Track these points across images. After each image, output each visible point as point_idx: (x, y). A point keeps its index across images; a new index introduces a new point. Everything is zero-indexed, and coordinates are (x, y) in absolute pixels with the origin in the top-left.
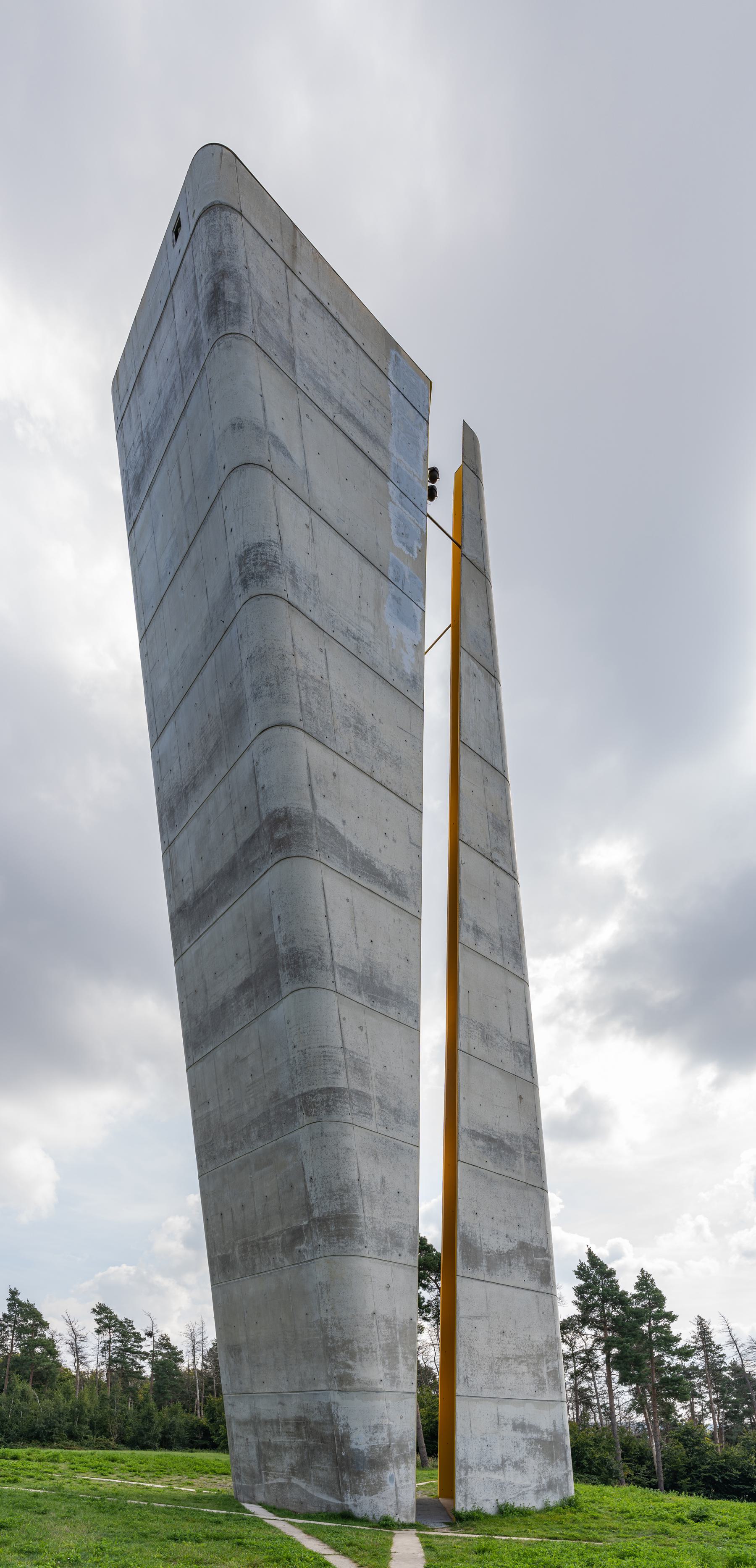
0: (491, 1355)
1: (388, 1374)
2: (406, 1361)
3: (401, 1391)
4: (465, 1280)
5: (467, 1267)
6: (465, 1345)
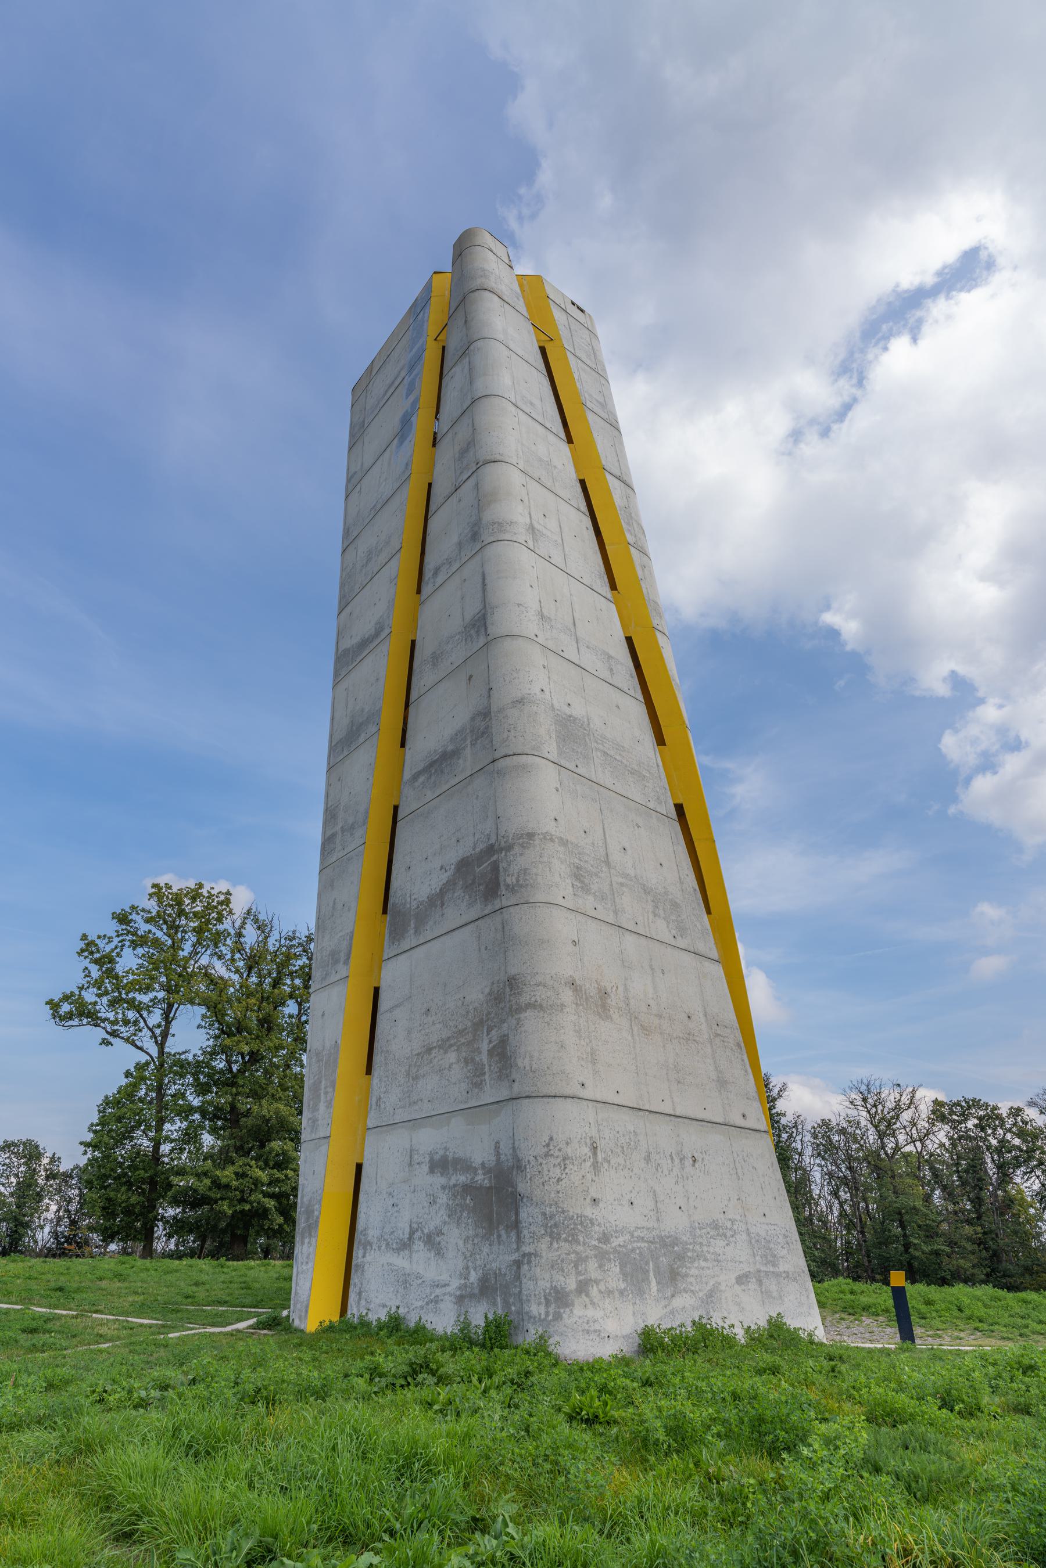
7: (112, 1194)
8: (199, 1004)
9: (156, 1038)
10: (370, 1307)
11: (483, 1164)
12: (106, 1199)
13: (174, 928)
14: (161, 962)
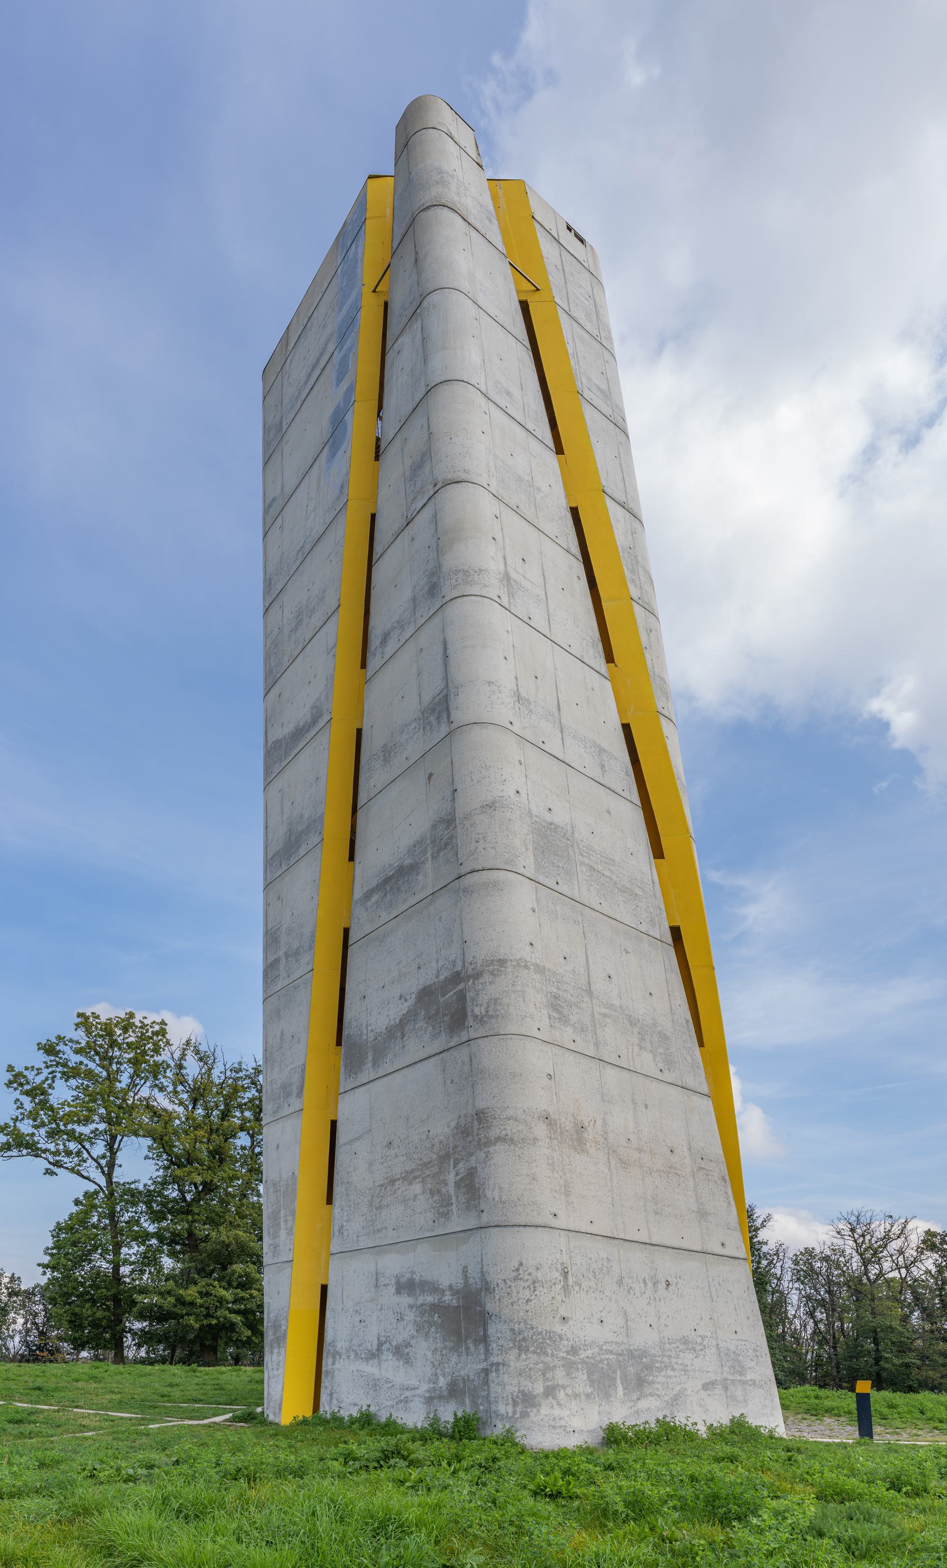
7: (77, 1310)
8: (144, 1136)
9: (102, 1168)
10: (342, 1406)
11: (451, 1287)
12: (72, 1314)
13: (107, 1060)
14: (98, 1094)
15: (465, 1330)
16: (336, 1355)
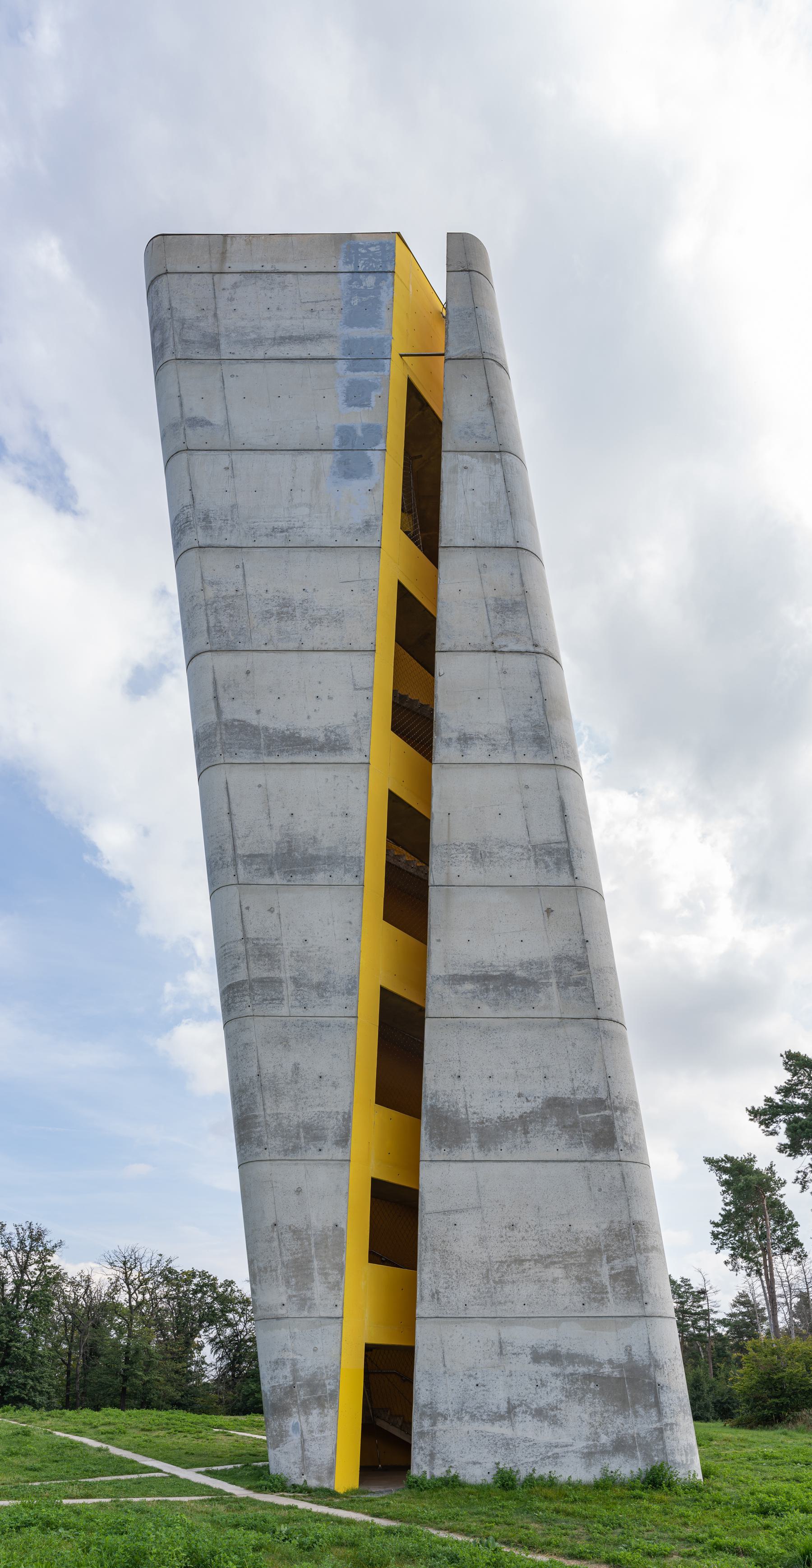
0: (486, 1259)
1: (294, 1296)
2: (326, 1279)
3: (316, 1316)
4: (434, 1166)
5: (440, 1148)
6: (434, 1250)
10: (452, 1465)
15: (632, 1397)
16: (435, 1416)
